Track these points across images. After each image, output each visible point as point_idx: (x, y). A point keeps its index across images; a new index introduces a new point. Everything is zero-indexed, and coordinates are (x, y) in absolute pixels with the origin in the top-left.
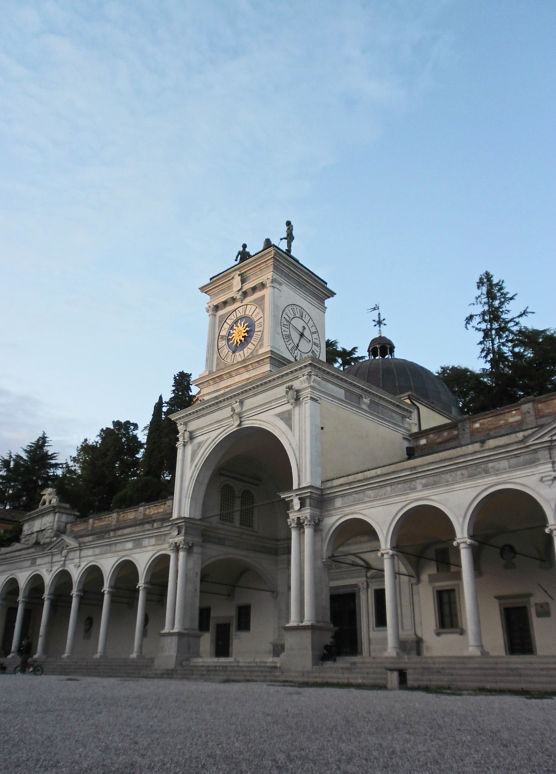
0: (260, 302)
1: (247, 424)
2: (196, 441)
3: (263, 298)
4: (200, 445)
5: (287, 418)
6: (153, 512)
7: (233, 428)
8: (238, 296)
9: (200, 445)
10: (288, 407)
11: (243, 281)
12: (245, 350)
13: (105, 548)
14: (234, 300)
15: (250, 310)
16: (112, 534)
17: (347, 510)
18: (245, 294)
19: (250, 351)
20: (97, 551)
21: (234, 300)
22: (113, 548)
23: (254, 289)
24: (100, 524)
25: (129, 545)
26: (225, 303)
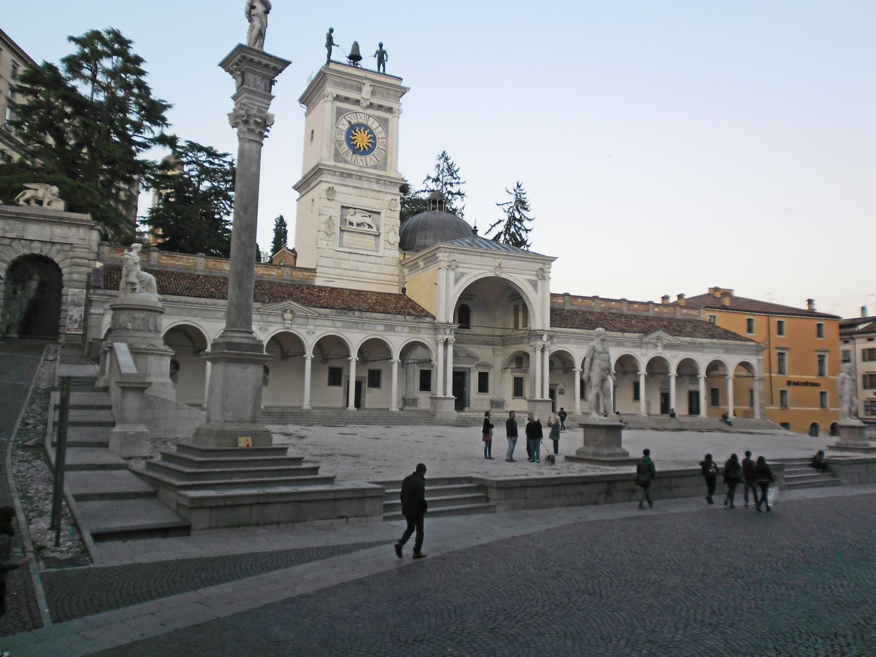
0: (384, 123)
1: (503, 276)
2: (458, 270)
3: (386, 121)
4: (463, 275)
5: (534, 285)
6: (261, 272)
7: (492, 274)
8: (364, 104)
9: (463, 275)
10: (534, 278)
11: (373, 93)
12: (368, 159)
13: (349, 324)
14: (357, 102)
15: (373, 124)
16: (357, 313)
17: (560, 345)
18: (371, 106)
19: (372, 163)
20: (339, 324)
21: (357, 102)
22: (360, 326)
23: (380, 107)
24: (172, 262)
25: (381, 328)
26: (346, 99)
